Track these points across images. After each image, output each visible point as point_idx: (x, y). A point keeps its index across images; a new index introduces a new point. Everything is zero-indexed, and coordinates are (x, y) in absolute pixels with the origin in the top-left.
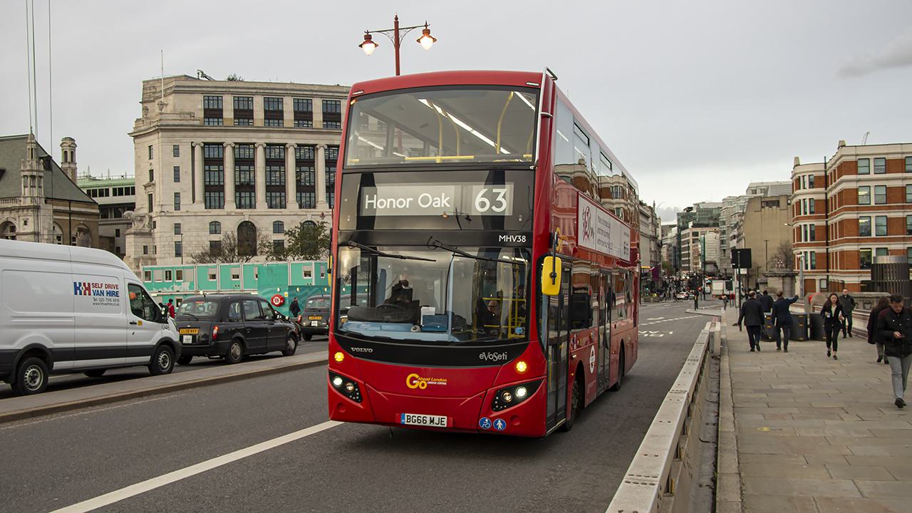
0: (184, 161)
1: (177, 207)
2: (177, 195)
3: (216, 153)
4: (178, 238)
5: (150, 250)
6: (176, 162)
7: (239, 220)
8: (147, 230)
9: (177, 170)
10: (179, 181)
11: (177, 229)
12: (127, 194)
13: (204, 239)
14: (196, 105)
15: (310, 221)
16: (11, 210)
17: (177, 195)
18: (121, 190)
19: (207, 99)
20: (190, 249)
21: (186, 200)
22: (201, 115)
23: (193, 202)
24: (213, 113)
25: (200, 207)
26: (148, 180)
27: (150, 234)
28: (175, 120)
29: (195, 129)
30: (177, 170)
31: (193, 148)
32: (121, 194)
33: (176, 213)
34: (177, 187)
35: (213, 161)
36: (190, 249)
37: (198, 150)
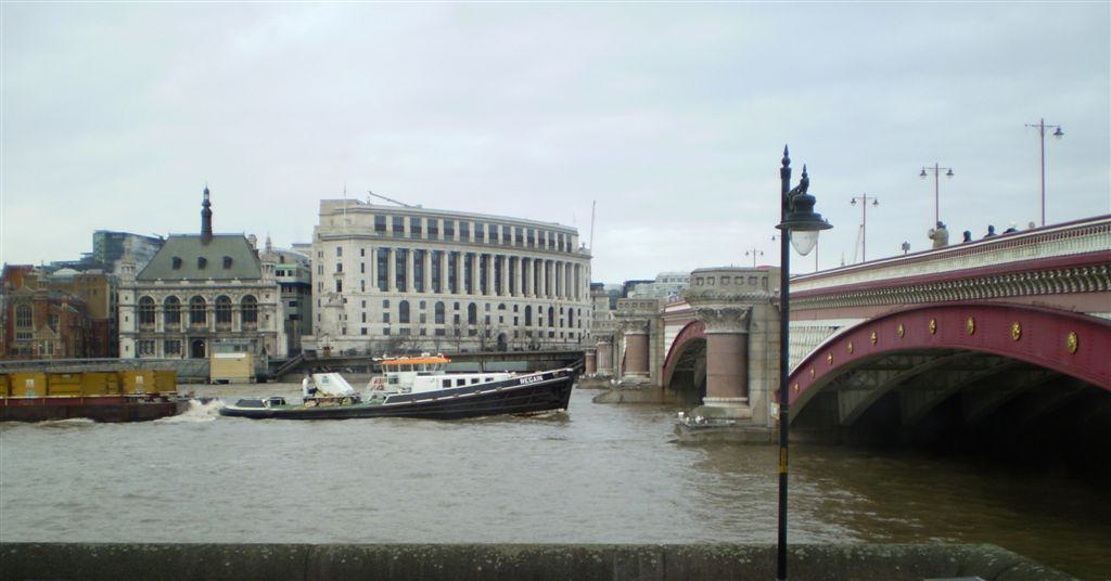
0: (367, 259)
1: (363, 290)
2: (363, 282)
5: (343, 317)
6: (363, 259)
7: (401, 299)
8: (340, 304)
9: (363, 265)
11: (364, 303)
14: (370, 221)
16: (253, 288)
17: (363, 282)
19: (377, 218)
24: (380, 227)
25: (377, 290)
26: (335, 270)
27: (342, 307)
29: (374, 239)
30: (363, 265)
34: (362, 277)
35: (383, 260)
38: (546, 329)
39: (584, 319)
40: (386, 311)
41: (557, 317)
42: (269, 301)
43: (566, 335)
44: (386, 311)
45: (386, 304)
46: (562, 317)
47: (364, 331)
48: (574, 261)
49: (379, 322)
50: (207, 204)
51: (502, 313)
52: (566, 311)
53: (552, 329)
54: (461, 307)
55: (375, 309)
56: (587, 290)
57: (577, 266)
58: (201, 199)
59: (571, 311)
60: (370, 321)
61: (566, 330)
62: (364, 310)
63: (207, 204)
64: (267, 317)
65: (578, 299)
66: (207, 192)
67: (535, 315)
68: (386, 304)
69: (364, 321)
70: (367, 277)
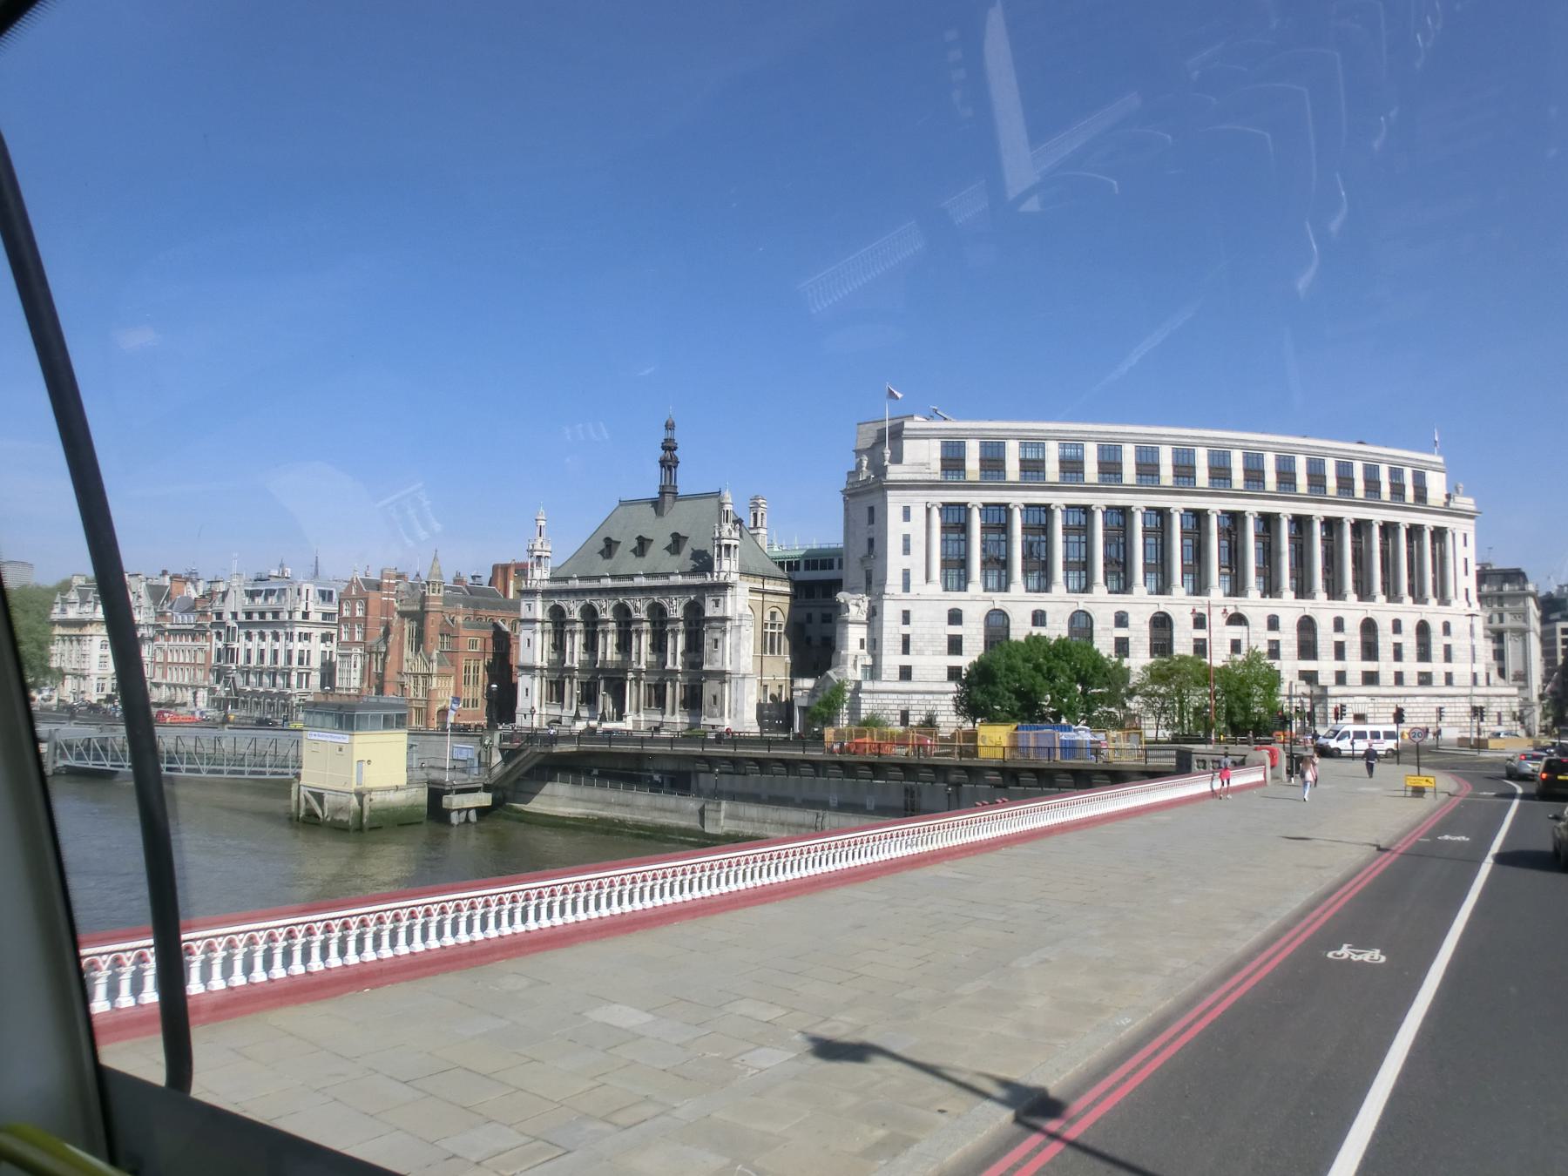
1: (906, 587)
2: (906, 574)
3: (956, 517)
4: (906, 630)
10: (909, 554)
12: (823, 567)
13: (941, 631)
15: (1084, 611)
18: (815, 562)
20: (922, 644)
21: (917, 578)
22: (937, 466)
23: (927, 582)
24: (953, 461)
25: (936, 587)
28: (905, 473)
31: (928, 511)
32: (815, 568)
33: (906, 596)
36: (922, 644)
37: (935, 514)
38: (1355, 665)
39: (1460, 642)
40: (955, 630)
41: (1386, 641)
42: (719, 613)
43: (1411, 678)
44: (955, 630)
45: (955, 617)
46: (1397, 638)
47: (906, 673)
48: (1429, 522)
49: (940, 653)
50: (669, 446)
51: (1237, 632)
52: (1409, 627)
53: (1370, 666)
54: (1132, 620)
55: (930, 627)
56: (1470, 582)
57: (1439, 534)
58: (662, 435)
59: (1423, 629)
60: (920, 653)
61: (1411, 666)
62: (906, 630)
63: (669, 446)
64: (716, 641)
65: (1443, 599)
66: (669, 426)
67: (1326, 638)
68: (955, 617)
69: (906, 650)
70: (916, 561)
